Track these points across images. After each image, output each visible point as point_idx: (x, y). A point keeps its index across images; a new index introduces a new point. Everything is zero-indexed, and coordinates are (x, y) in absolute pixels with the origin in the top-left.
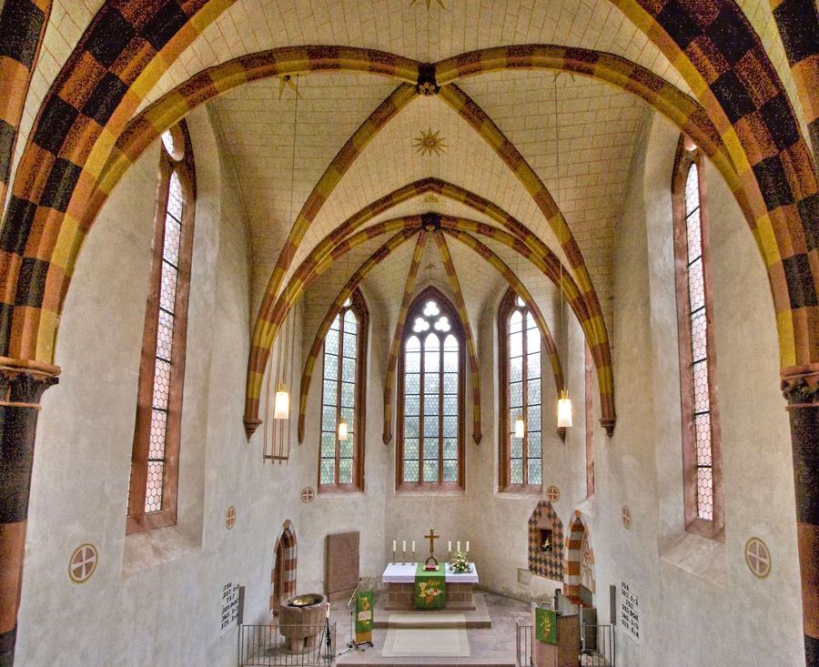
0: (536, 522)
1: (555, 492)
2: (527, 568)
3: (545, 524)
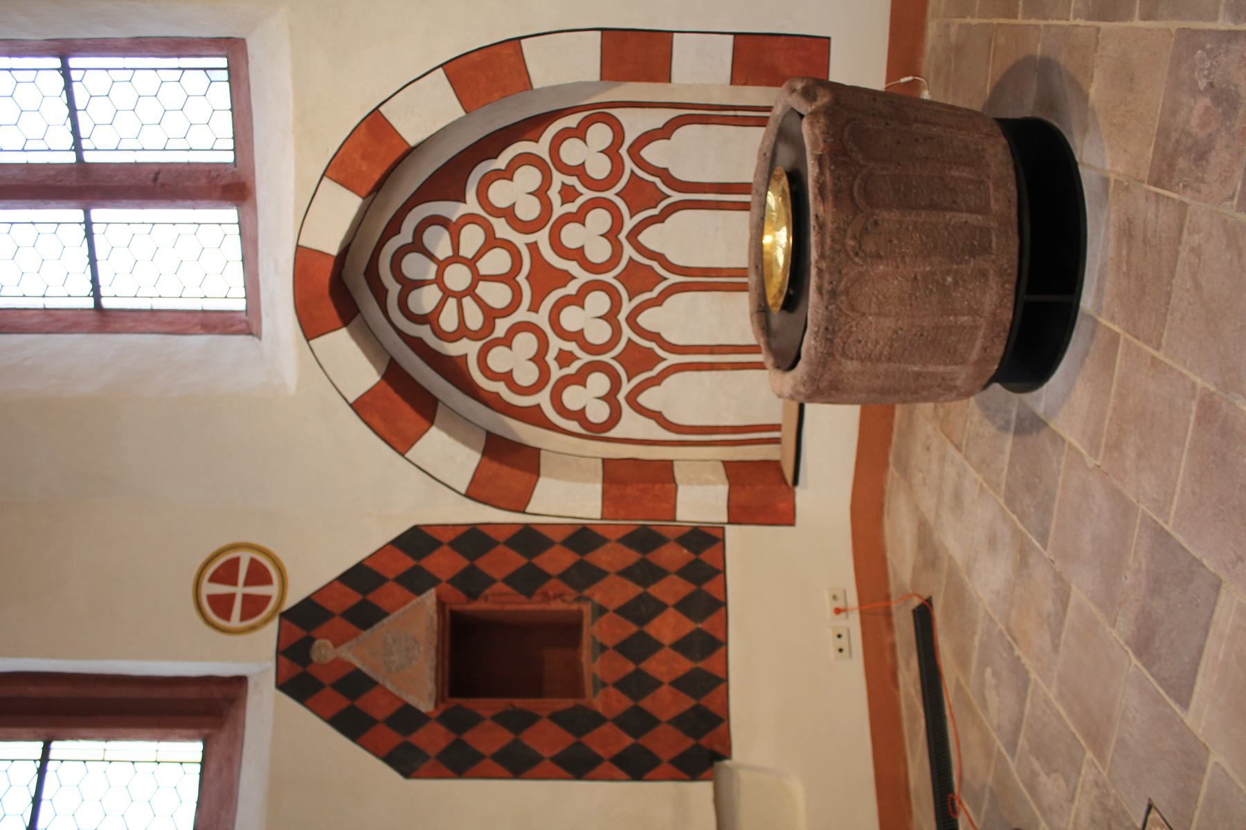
0: (407, 718)
1: (227, 573)
2: (701, 790)
3: (404, 655)
